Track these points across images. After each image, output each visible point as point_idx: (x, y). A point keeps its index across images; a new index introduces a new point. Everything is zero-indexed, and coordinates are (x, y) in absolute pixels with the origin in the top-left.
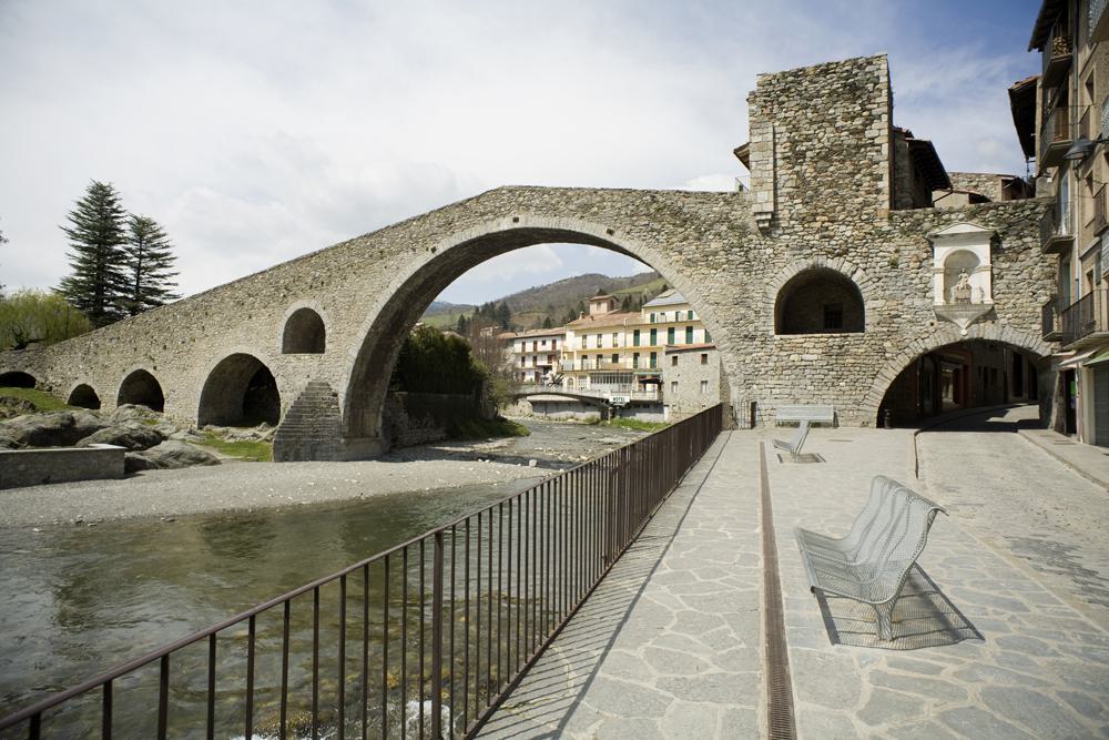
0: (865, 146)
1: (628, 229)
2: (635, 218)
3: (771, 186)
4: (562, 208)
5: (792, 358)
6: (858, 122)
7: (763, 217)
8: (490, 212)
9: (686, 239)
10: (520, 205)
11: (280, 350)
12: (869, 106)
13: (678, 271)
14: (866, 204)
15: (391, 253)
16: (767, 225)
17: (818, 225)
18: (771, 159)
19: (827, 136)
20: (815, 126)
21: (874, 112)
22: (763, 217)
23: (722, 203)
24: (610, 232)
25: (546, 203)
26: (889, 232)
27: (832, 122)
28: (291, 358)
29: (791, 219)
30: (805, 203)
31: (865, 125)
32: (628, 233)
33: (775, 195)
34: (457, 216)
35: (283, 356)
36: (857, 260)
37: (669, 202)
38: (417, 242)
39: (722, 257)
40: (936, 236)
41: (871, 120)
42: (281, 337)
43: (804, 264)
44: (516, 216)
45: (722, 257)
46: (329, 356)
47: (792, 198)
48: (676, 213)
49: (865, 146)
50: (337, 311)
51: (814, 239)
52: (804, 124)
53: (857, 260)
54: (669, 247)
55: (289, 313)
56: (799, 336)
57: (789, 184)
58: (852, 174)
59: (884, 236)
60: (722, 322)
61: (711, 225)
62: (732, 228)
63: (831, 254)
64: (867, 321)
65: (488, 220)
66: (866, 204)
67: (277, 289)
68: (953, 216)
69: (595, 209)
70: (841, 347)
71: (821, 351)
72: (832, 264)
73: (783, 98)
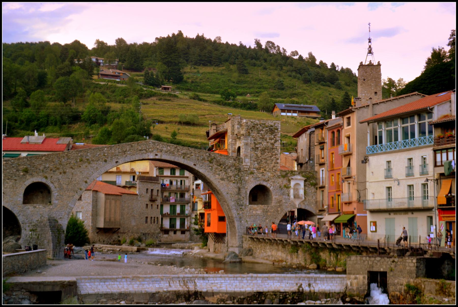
0: (274, 149)
1: (201, 165)
2: (203, 161)
3: (249, 157)
4: (176, 153)
5: (253, 212)
6: (273, 141)
7: (247, 167)
8: (144, 150)
9: (221, 171)
10: (158, 149)
12: (275, 137)
13: (219, 182)
14: (274, 166)
15: (93, 161)
16: (247, 169)
17: (261, 171)
18: (249, 149)
19: (265, 144)
20: (261, 140)
21: (277, 139)
22: (247, 167)
23: (233, 160)
24: (195, 165)
25: (169, 150)
26: (280, 176)
27: (266, 140)
28: (28, 206)
29: (254, 168)
30: (257, 164)
31: (275, 142)
32: (201, 166)
33: (251, 160)
34: (128, 150)
35: (23, 205)
36: (271, 183)
37: (215, 157)
38: (108, 158)
39: (232, 178)
40: (292, 179)
41: (276, 141)
42: (22, 196)
43: (258, 183)
44: (157, 154)
45: (232, 178)
46: (56, 206)
47: (254, 162)
48: (217, 161)
49: (274, 149)
51: (260, 175)
52: (258, 138)
53: (271, 183)
54: (215, 173)
56: (255, 205)
57: (254, 157)
58: (271, 157)
59: (279, 177)
60: (233, 200)
61: (229, 167)
62: (236, 169)
63: (264, 180)
64: (273, 202)
65: (143, 153)
66: (274, 166)
67: (18, 170)
68: (295, 173)
69: (189, 156)
70: (267, 209)
72: (265, 184)
73: (252, 129)
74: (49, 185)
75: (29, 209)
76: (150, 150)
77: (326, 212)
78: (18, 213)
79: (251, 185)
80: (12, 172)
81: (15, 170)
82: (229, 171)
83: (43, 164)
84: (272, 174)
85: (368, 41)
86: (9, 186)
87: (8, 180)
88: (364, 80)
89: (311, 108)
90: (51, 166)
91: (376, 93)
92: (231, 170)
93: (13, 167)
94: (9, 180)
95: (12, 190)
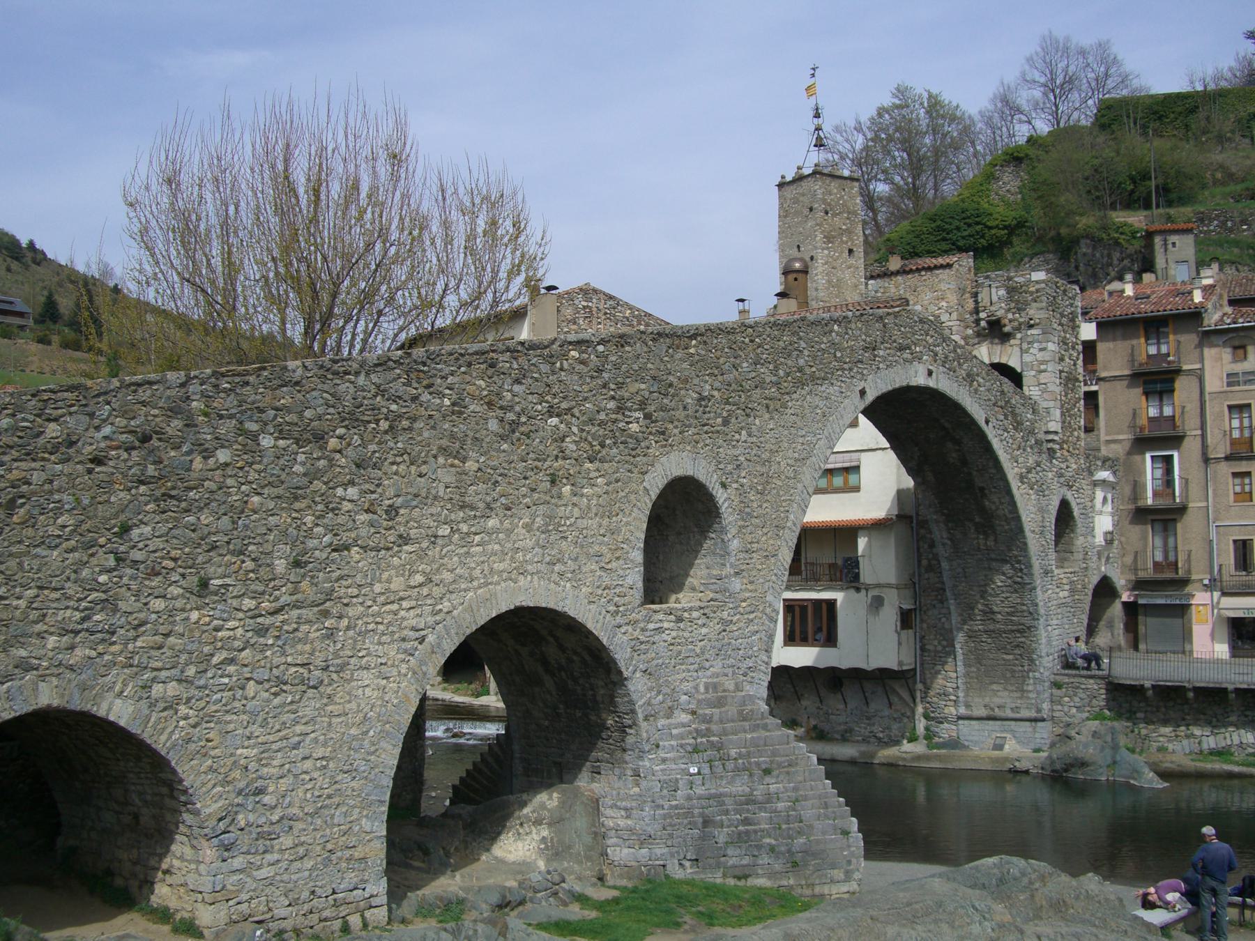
11: (637, 595)
24: (987, 422)
42: (638, 556)
44: (931, 367)
48: (1014, 414)
50: (742, 491)
55: (656, 482)
71: (1067, 587)
74: (714, 493)
75: (659, 630)
76: (918, 349)
77: (1197, 585)
78: (632, 658)
79: (1055, 503)
80: (602, 416)
81: (612, 405)
82: (1029, 450)
83: (696, 381)
84: (1076, 463)
85: (812, 113)
86: (594, 502)
87: (588, 465)
88: (827, 213)
89: (11, 303)
90: (715, 393)
91: (851, 251)
92: (1031, 448)
93: (604, 386)
94: (597, 464)
95: (605, 522)
